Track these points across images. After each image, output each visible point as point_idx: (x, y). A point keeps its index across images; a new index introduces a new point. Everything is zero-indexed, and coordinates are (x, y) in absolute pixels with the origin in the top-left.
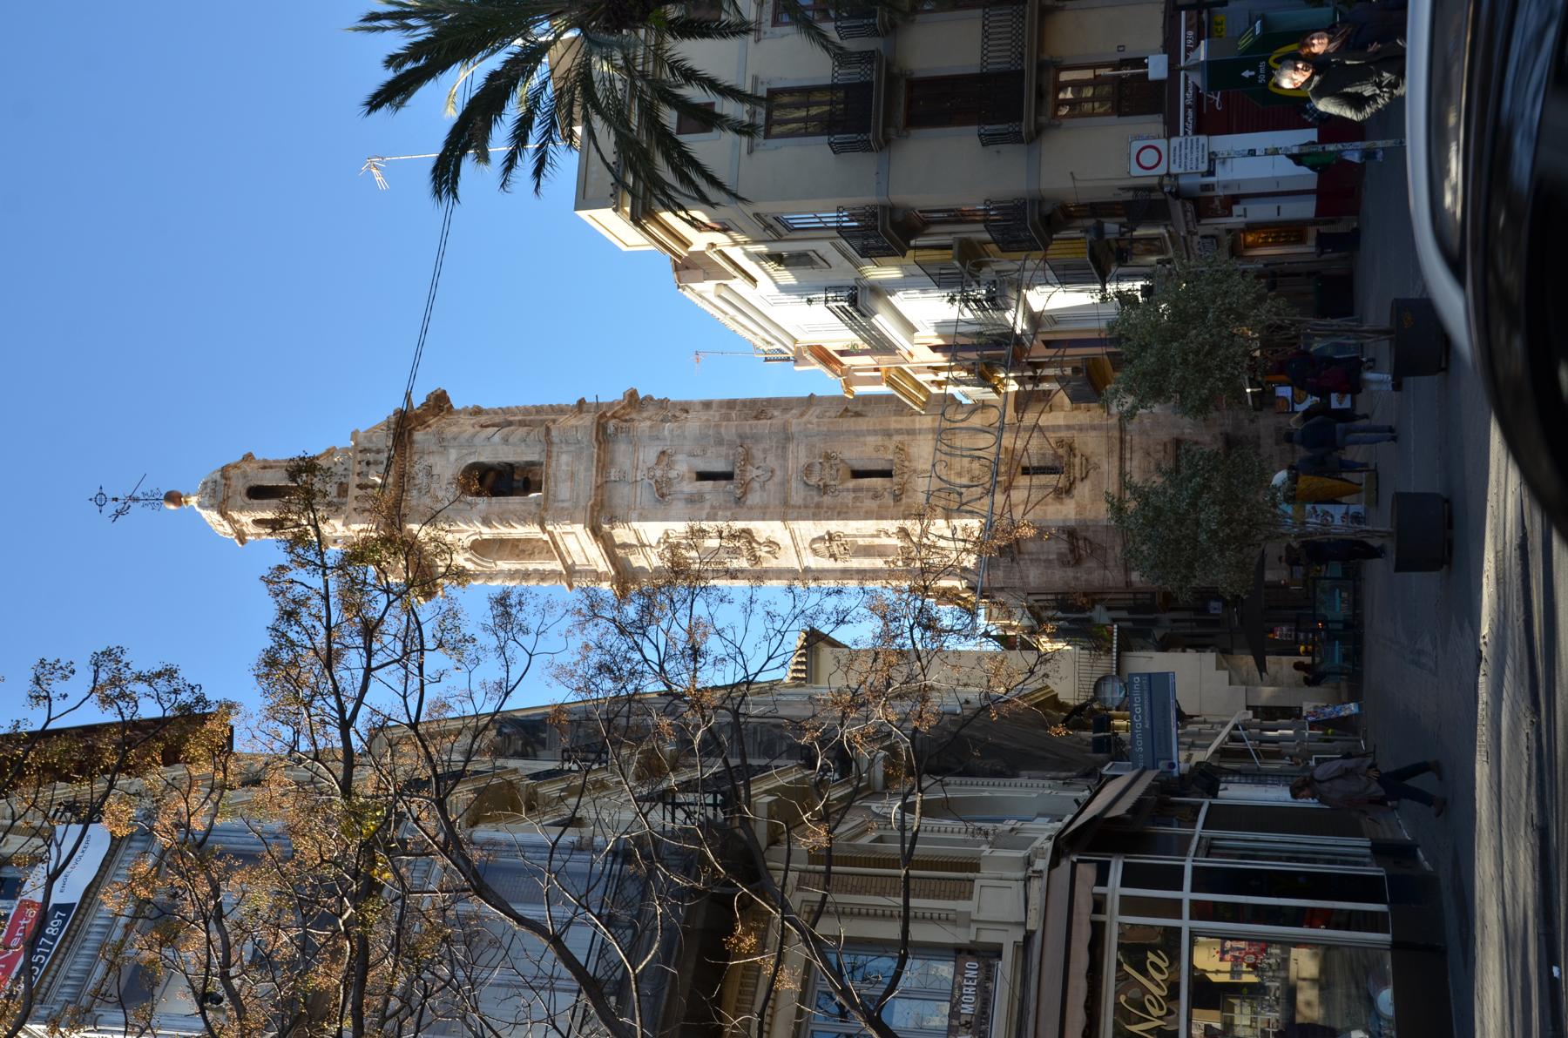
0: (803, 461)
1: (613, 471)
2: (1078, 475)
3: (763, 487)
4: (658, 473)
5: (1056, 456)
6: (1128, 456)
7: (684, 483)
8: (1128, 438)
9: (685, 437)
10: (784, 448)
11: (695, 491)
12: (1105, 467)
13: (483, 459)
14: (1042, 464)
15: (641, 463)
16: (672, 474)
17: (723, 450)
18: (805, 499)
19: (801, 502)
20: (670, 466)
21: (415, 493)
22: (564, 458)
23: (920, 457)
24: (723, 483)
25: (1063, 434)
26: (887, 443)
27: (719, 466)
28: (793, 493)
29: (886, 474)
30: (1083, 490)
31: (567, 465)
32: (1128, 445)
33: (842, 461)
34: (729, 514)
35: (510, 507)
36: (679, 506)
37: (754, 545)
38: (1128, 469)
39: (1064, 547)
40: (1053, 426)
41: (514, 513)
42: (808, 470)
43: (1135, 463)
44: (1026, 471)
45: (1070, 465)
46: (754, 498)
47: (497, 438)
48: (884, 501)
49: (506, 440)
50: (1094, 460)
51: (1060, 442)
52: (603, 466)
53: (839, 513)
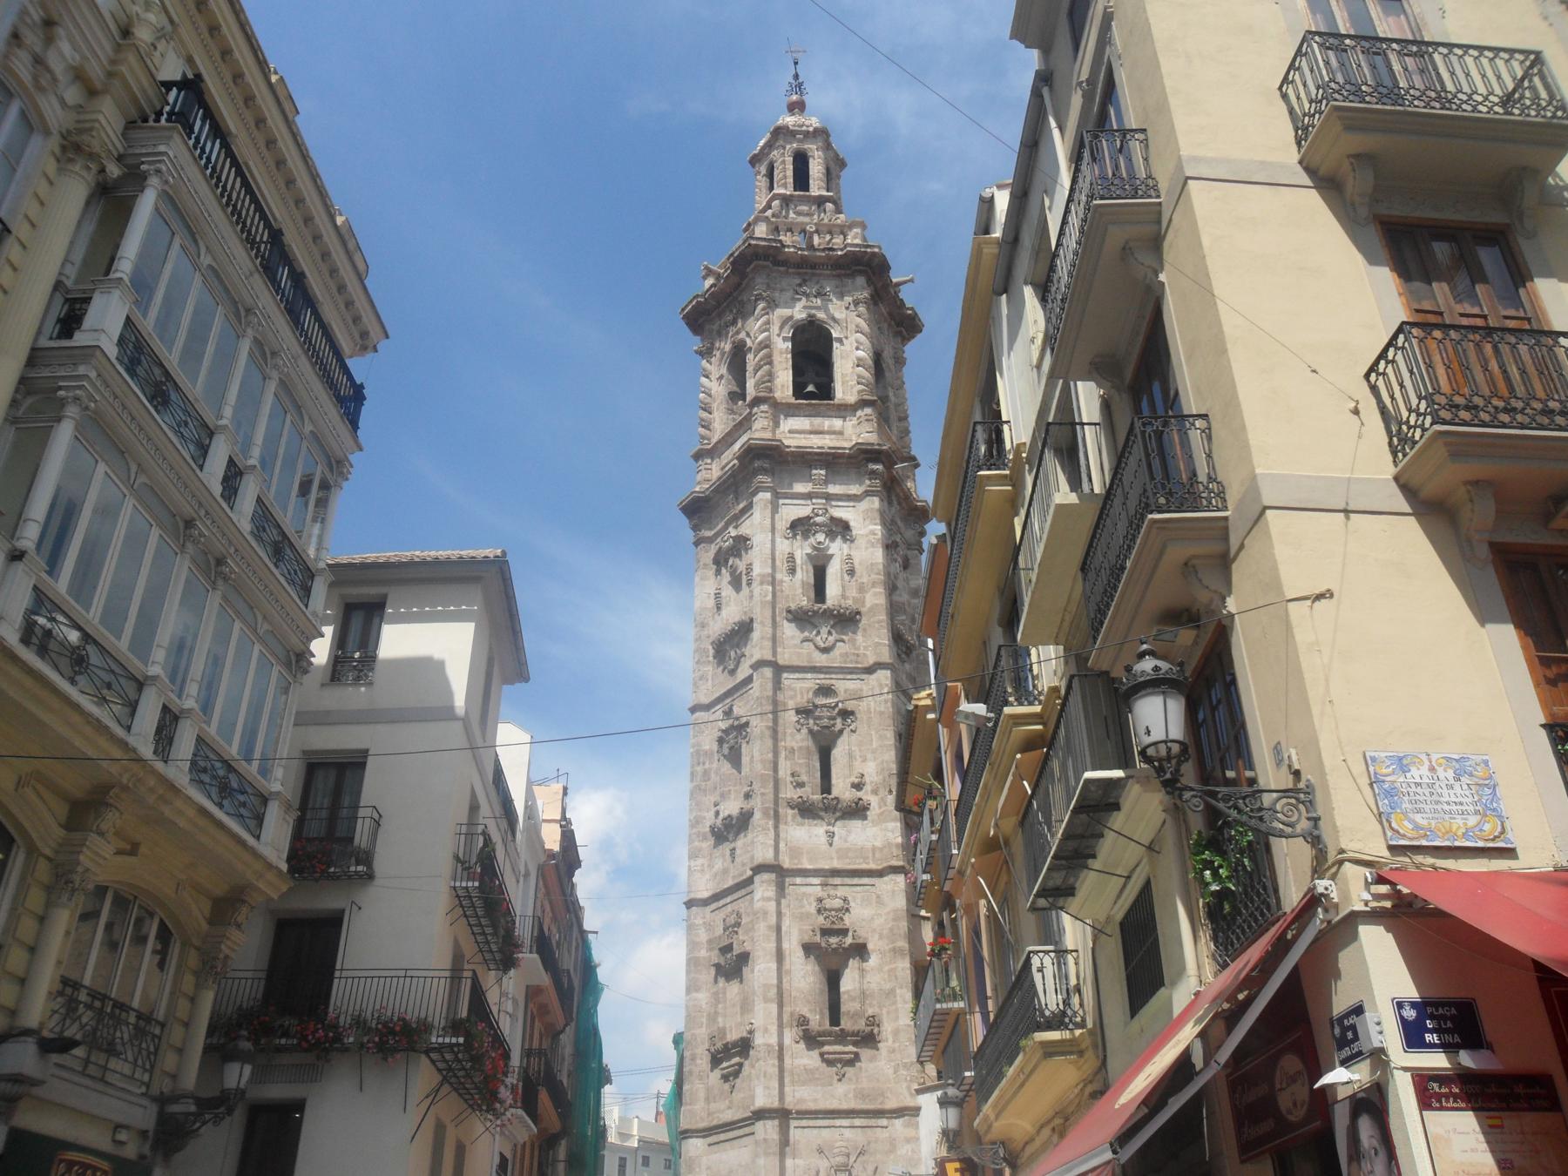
0: (844, 686)
1: (823, 472)
2: (827, 1048)
3: (806, 640)
4: (819, 519)
5: (855, 1016)
6: (857, 1122)
7: (809, 551)
8: (884, 1122)
9: (867, 548)
10: (857, 662)
11: (798, 561)
12: (841, 1089)
13: (835, 345)
14: (844, 998)
15: (834, 503)
16: (821, 537)
17: (853, 593)
18: (790, 688)
19: (786, 682)
20: (831, 535)
21: (798, 281)
22: (837, 423)
23: (849, 832)
24: (812, 595)
25: (887, 1029)
26: (868, 788)
27: (833, 590)
28: (797, 675)
29: (826, 787)
30: (807, 1059)
31: (830, 426)
32: (872, 1122)
33: (841, 732)
34: (769, 597)
35: (781, 373)
36: (783, 546)
37: (736, 640)
38: (838, 1122)
39: (733, 1036)
40: (896, 1010)
41: (771, 376)
42: (826, 691)
43: (848, 1133)
44: (833, 980)
45: (842, 1037)
46: (789, 630)
47: (861, 353)
48: (790, 787)
49: (860, 363)
50: (850, 1071)
51: (873, 1021)
52: (835, 463)
53: (768, 728)
